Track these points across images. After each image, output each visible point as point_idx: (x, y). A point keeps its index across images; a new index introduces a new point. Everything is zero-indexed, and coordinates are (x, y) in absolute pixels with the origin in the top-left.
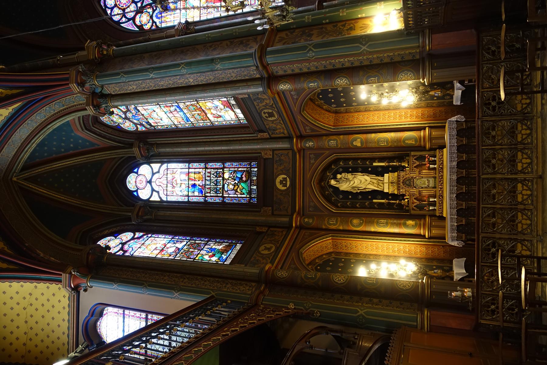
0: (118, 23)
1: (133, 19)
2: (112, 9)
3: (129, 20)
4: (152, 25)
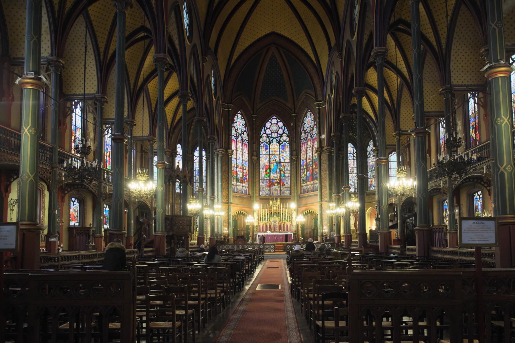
0: (265, 126)
1: (265, 133)
2: (271, 122)
3: (265, 131)
4: (261, 142)
